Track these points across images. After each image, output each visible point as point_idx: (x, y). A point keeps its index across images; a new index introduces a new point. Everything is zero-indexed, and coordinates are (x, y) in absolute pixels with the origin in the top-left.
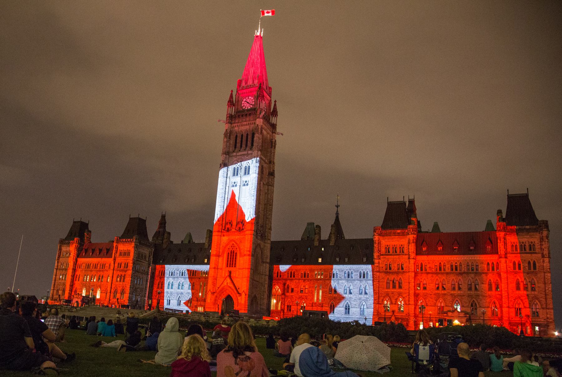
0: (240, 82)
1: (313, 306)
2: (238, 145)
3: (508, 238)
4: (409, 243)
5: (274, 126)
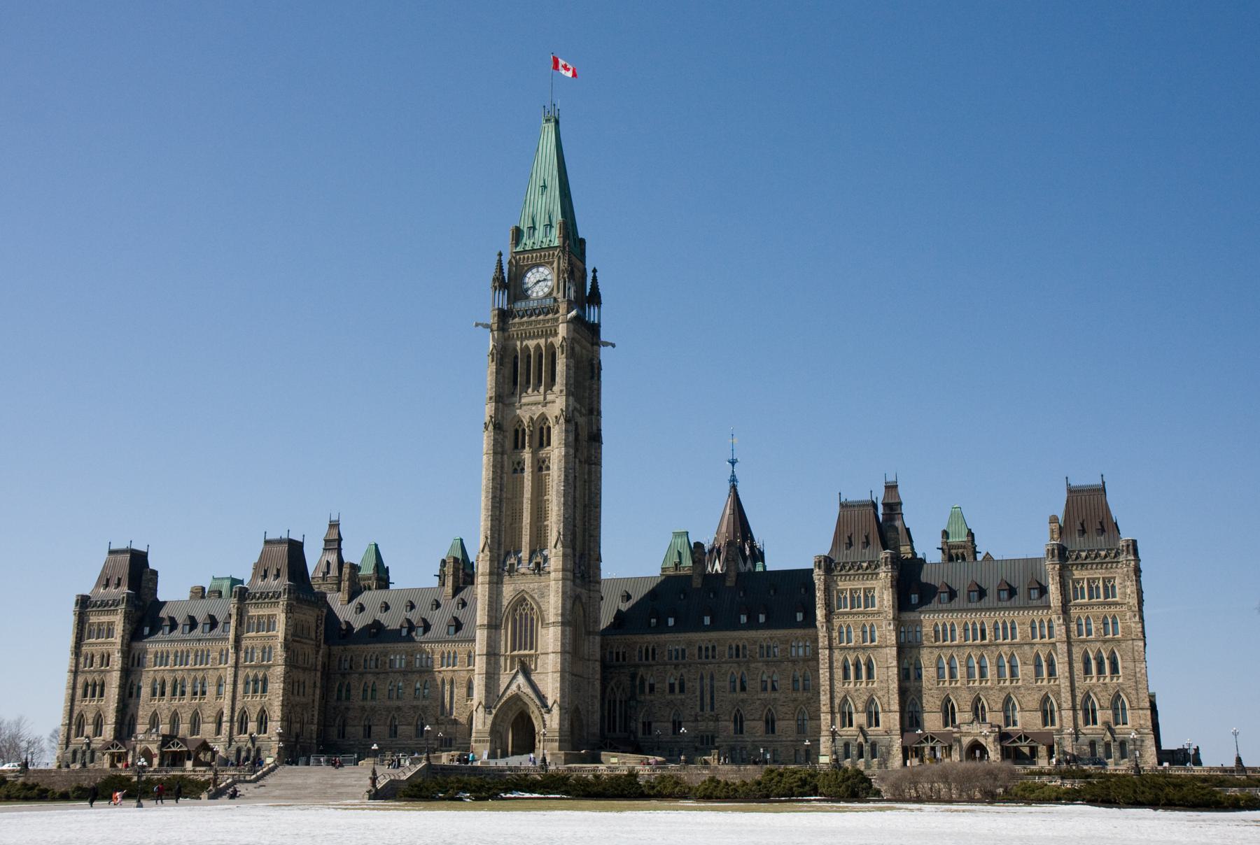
1: (696, 720)
5: (595, 329)
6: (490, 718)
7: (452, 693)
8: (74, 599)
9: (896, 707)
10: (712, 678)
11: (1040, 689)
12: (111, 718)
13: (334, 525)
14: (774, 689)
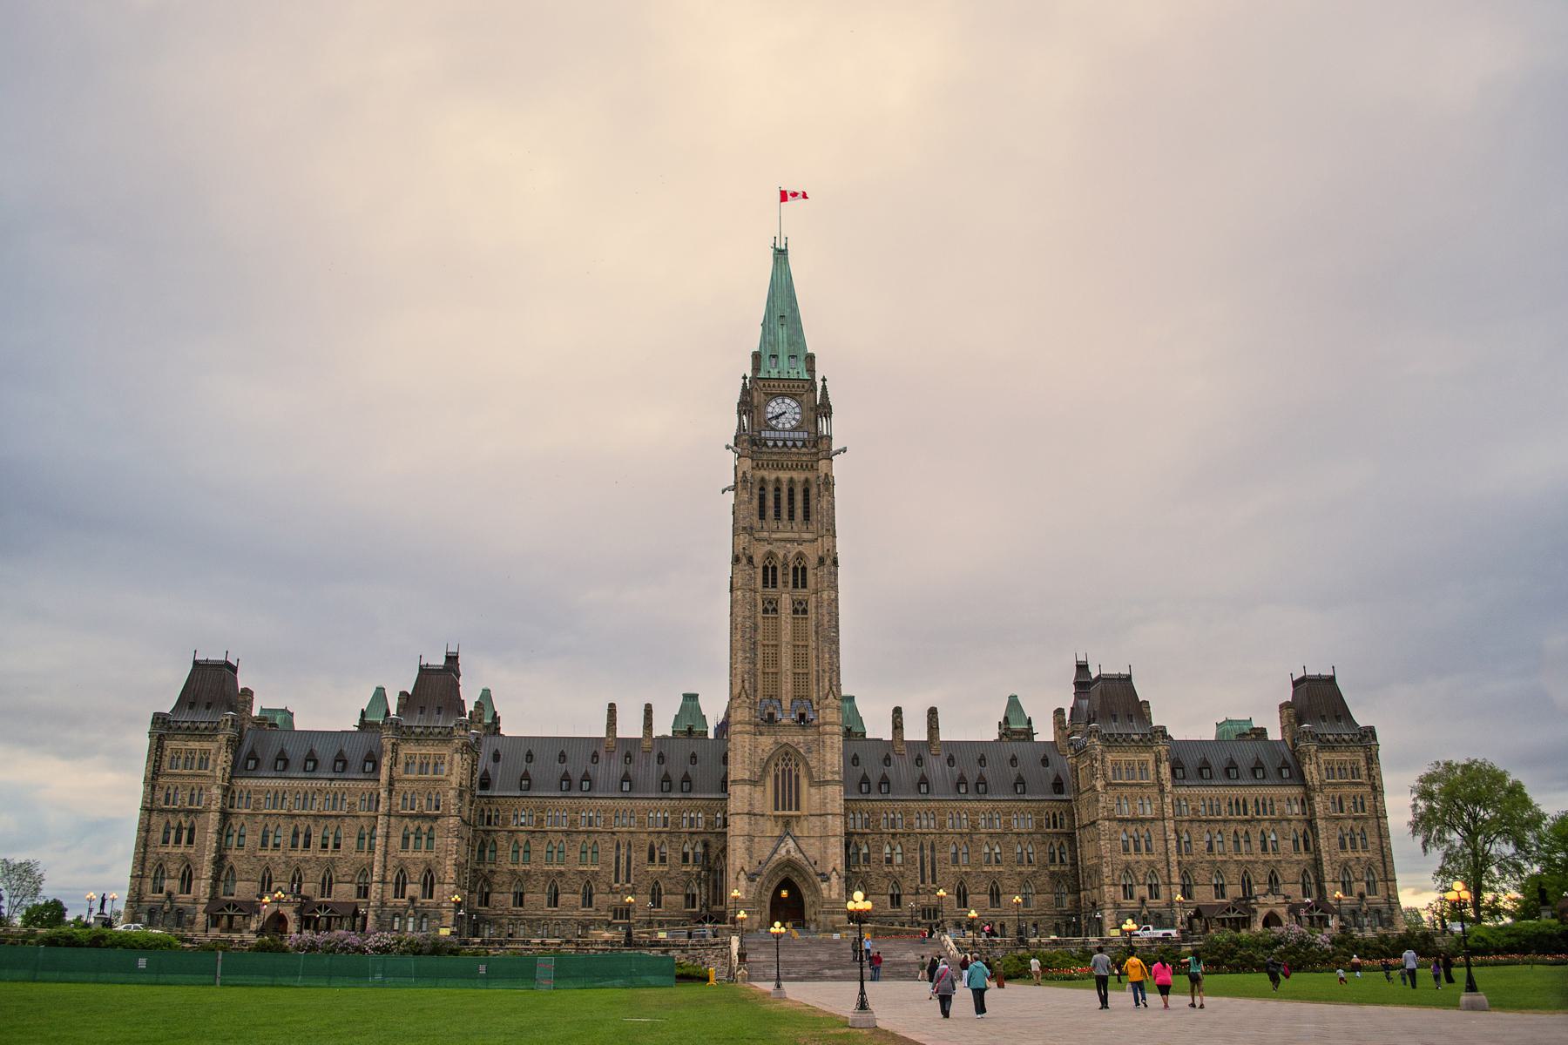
0: (756, 357)
2: (771, 512)
4: (1158, 761)
6: (754, 887)
7: (629, 858)
9: (1176, 880)
10: (933, 849)
11: (1298, 862)
12: (206, 871)
13: (452, 659)
14: (997, 861)
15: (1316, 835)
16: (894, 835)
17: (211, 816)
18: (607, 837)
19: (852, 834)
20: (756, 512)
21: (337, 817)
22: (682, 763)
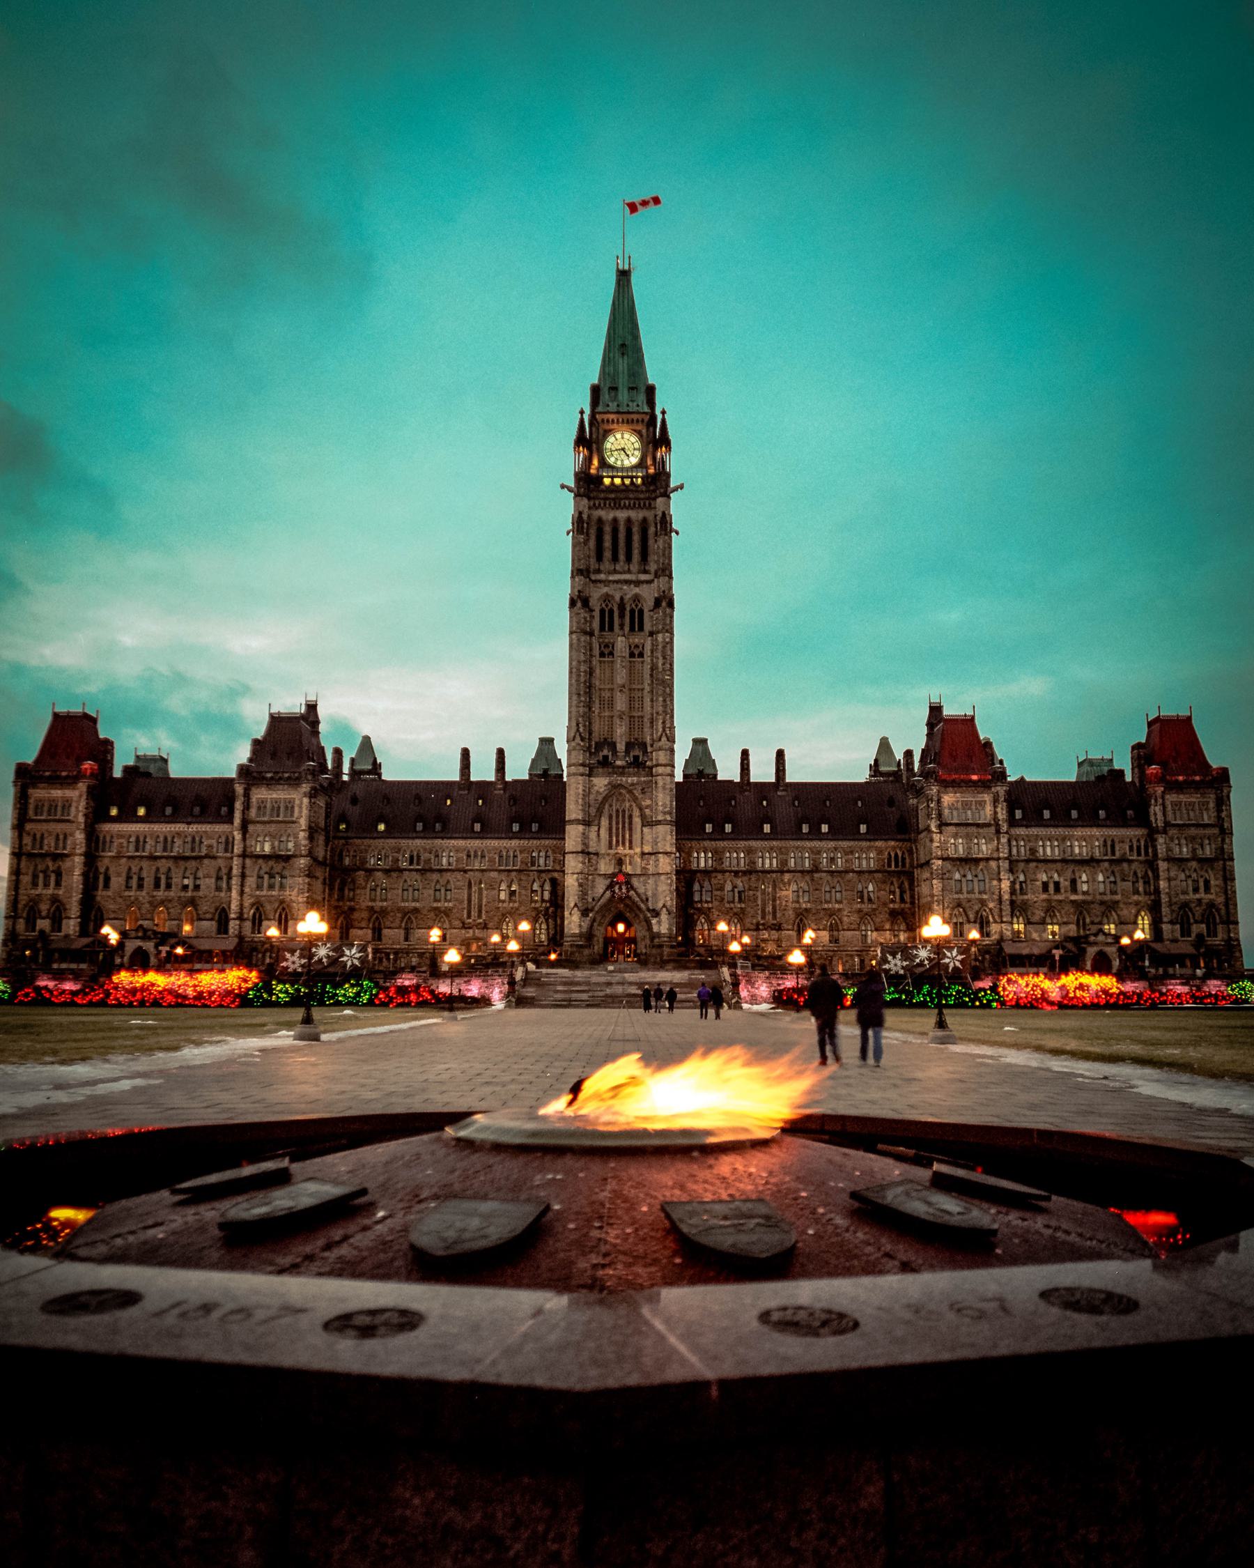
0: (595, 390)
2: (608, 554)
3: (1167, 797)
4: (995, 801)
8: (13, 768)
12: (74, 909)
15: (1157, 878)
16: (736, 873)
17: (77, 859)
18: (459, 875)
19: (694, 872)
20: (593, 554)
21: (195, 858)
22: (530, 806)
